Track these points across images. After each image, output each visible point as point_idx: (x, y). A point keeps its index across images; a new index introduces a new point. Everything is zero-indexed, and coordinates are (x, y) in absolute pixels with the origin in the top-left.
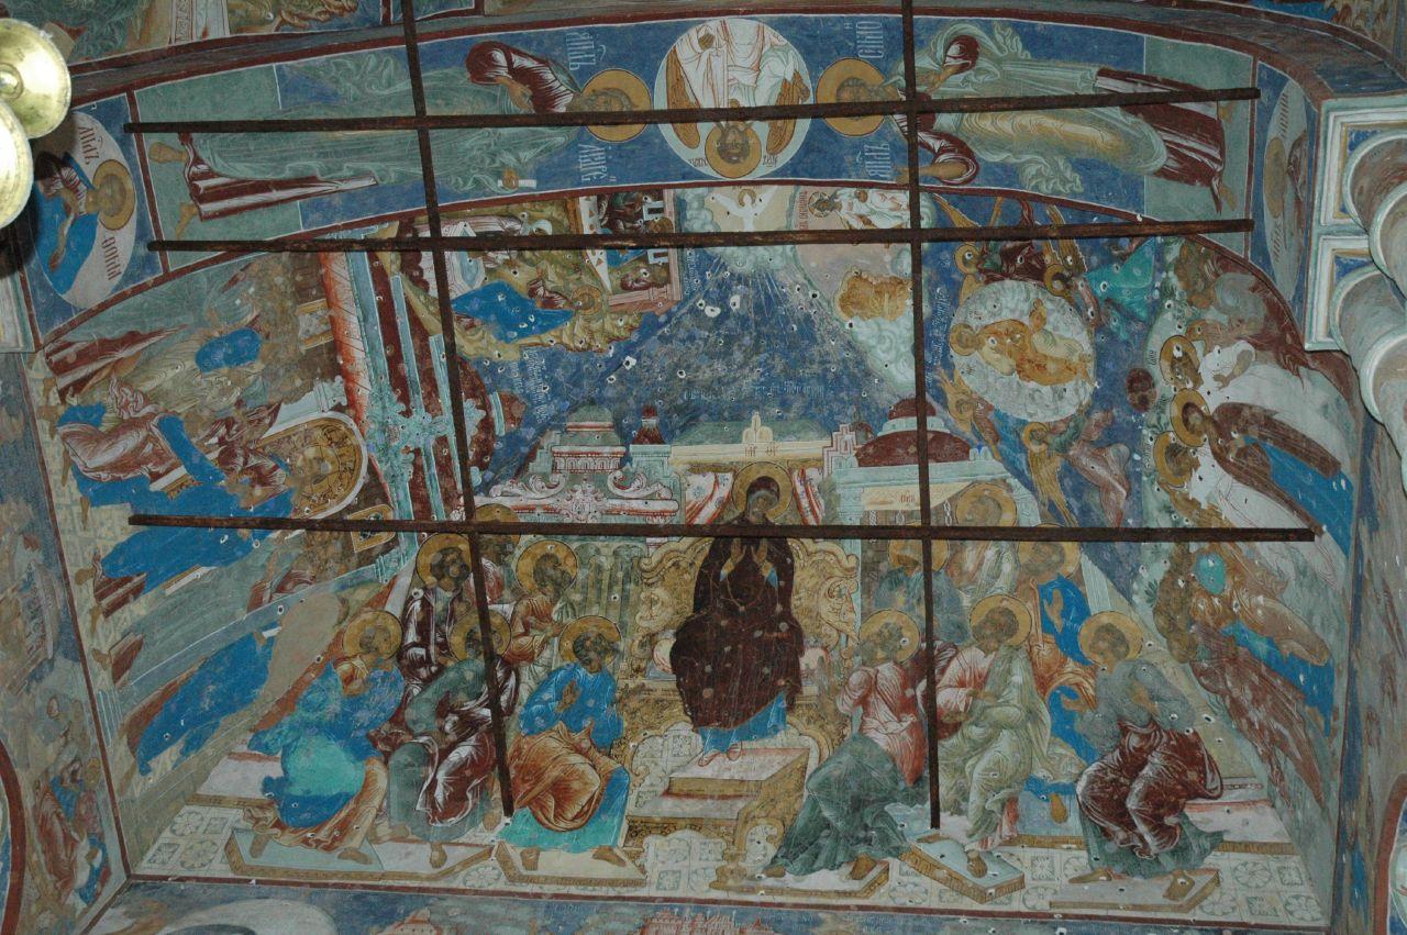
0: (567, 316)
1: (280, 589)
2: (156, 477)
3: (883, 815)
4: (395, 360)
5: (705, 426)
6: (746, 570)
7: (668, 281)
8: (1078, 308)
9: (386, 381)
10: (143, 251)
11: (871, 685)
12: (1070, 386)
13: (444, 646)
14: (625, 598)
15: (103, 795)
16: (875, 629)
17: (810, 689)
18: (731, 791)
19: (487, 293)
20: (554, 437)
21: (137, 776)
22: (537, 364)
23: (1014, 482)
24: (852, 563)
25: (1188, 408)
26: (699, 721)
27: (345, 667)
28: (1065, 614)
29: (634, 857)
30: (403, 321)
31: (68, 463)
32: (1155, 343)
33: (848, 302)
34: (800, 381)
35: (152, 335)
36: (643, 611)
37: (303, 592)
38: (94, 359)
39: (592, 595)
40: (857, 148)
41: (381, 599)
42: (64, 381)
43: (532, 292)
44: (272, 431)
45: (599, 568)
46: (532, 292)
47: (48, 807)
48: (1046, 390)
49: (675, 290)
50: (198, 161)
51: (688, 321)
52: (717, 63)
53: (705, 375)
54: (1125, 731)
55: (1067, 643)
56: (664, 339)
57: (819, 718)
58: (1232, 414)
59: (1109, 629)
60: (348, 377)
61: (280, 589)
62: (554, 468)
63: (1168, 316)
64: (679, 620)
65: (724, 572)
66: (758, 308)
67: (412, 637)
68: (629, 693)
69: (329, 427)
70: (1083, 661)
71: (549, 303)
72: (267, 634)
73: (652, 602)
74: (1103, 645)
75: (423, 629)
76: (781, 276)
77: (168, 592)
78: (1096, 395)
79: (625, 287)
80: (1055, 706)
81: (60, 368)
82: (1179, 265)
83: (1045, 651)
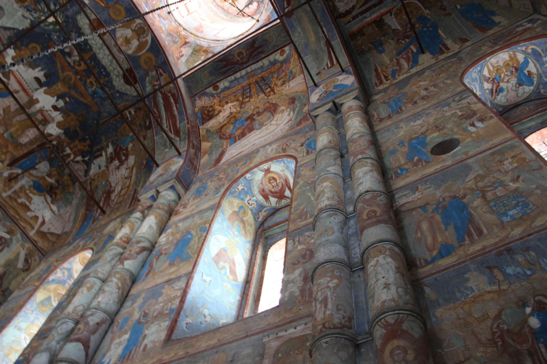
1: (445, 9)
2: (412, 52)
9: (381, 6)
15: (504, 31)
31: (406, 73)
35: (375, 65)
38: (380, 76)
42: (384, 81)
44: (400, 28)
47: (501, 43)
50: (324, 69)
60: (383, 15)
61: (445, 9)
69: (396, 15)
72: (459, 7)
77: (445, 37)
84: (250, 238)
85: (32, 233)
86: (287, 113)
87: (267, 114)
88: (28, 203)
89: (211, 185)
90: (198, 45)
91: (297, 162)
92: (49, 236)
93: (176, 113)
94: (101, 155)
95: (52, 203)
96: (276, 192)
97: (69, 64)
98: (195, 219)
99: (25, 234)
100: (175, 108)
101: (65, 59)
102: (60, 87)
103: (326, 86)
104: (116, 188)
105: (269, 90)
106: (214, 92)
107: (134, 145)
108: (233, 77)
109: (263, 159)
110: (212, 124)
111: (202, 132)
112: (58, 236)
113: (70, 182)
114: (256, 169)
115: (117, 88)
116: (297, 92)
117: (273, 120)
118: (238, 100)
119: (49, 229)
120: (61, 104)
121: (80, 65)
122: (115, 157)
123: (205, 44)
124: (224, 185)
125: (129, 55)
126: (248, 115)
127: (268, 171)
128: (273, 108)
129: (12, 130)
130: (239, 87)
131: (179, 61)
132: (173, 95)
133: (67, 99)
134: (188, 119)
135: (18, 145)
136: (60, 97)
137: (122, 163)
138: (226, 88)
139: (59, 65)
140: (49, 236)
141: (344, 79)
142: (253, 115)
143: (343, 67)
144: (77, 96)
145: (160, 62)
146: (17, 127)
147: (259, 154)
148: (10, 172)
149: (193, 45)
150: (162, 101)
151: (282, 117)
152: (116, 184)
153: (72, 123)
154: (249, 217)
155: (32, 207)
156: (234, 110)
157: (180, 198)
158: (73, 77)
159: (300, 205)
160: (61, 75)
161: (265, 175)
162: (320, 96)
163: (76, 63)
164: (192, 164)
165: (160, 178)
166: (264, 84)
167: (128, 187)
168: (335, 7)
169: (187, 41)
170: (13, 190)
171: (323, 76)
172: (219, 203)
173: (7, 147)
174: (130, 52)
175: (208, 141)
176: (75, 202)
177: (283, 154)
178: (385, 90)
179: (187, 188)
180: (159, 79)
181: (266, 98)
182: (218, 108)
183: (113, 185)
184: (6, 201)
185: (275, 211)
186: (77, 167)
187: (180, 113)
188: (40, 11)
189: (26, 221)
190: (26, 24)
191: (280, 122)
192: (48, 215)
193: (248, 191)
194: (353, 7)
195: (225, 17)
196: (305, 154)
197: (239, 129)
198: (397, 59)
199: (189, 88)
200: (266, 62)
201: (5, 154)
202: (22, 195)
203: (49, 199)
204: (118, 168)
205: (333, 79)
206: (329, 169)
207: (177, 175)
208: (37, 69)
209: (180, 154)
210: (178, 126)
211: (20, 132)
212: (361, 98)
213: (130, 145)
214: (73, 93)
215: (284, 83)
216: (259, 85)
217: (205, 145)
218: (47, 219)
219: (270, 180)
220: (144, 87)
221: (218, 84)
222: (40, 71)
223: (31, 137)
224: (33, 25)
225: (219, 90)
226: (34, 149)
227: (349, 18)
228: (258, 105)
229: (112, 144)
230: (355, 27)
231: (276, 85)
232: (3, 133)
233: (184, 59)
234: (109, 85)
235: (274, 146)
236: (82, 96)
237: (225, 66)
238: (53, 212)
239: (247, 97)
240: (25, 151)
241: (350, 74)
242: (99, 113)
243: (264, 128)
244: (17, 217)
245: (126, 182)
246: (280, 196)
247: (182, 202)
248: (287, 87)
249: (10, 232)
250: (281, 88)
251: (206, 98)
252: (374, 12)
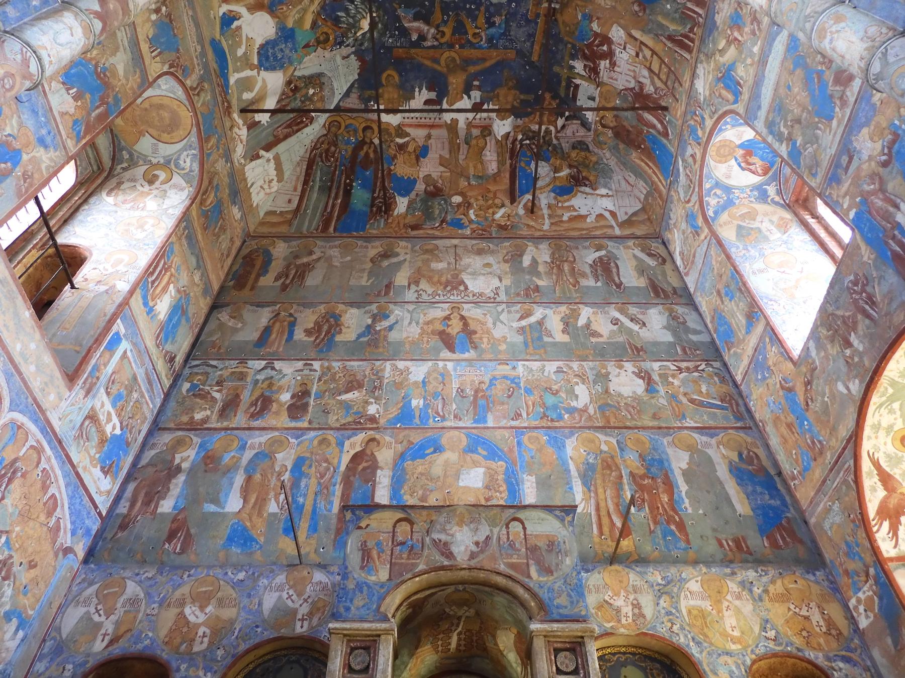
85: (617, 232)
88: (575, 214)
92: (634, 219)
94: (577, 87)
95: (595, 189)
97: (433, 47)
99: (611, 238)
102: (456, 81)
104: (641, 80)
107: (598, 18)
112: (643, 209)
113: (583, 153)
119: (626, 213)
120: (476, 95)
121: (443, 34)
122: (594, 63)
129: (472, 171)
133: (476, 83)
135: (495, 177)
136: (467, 90)
137: (610, 55)
139: (427, 63)
140: (634, 219)
144: (479, 68)
146: (471, 165)
148: (521, 206)
152: (634, 78)
153: (510, 99)
155: (583, 212)
158: (453, 54)
160: (441, 68)
163: (438, 36)
167: (654, 52)
170: (546, 216)
173: (489, 191)
176: (613, 162)
183: (632, 85)
184: (555, 231)
186: (569, 131)
188: (349, 30)
189: (596, 228)
190: (354, 62)
192: (608, 204)
201: (495, 197)
202: (559, 212)
203: (588, 190)
204: (613, 64)
208: (417, 93)
211: (479, 166)
214: (472, 69)
218: (611, 208)
222: (420, 92)
223: (495, 158)
224: (359, 55)
226: (511, 165)
229: (573, 60)
232: (469, 184)
236: (484, 60)
238: (607, 196)
240: (508, 176)
242: (520, 53)
244: (584, 232)
245: (644, 57)
249: (599, 248)
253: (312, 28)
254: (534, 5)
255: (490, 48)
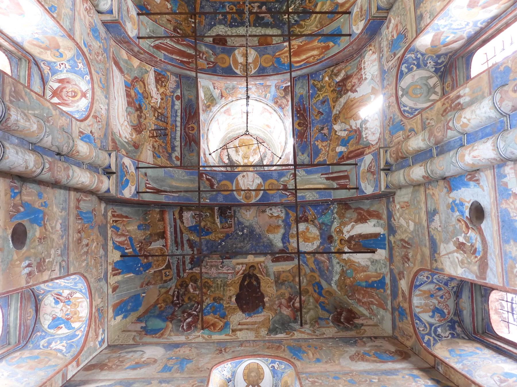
0: (211, 233)
1: (147, 284)
2: (127, 249)
3: (289, 325)
4: (176, 237)
5: (238, 257)
6: (250, 283)
7: (232, 227)
8: (316, 226)
9: (174, 242)
10: (135, 193)
11: (281, 304)
12: (315, 242)
13: (183, 300)
14: (224, 289)
15: (106, 320)
16: (279, 293)
17: (267, 305)
18: (255, 323)
19: (195, 226)
20: (207, 258)
21: (113, 319)
22: (204, 242)
23: (304, 265)
24: (272, 281)
25: (341, 240)
26: (244, 311)
27: (159, 305)
28: (318, 289)
29: (235, 335)
30: (178, 230)
31: (112, 237)
32: (333, 229)
33: (269, 231)
34: (259, 246)
36: (228, 292)
37: (151, 286)
39: (216, 289)
40: (272, 196)
41: (168, 291)
42: (114, 219)
43: (204, 227)
44: (150, 247)
45: (218, 284)
46: (204, 227)
47: (96, 314)
48: (310, 244)
49: (233, 229)
50: (147, 180)
51: (235, 236)
52: (245, 180)
53: (239, 246)
54: (336, 309)
55: (320, 294)
56: (231, 239)
57: (270, 309)
58: (351, 238)
59: (327, 291)
61: (147, 284)
62: (207, 265)
63: (335, 223)
64: (236, 293)
65: (245, 284)
66: (250, 232)
67: (175, 299)
68: (226, 307)
70: (324, 297)
71: (208, 230)
72: (143, 295)
73: (230, 290)
74: (327, 294)
75: (178, 297)
76: (255, 226)
78: (321, 243)
79: (223, 228)
80: (320, 305)
81: (113, 216)
82: (337, 213)
83: (316, 295)
84: (27, 46)
86: (128, 137)
87: (136, 122)
89: (96, 45)
90: (216, 104)
91: (77, 120)
93: (174, 57)
96: (61, 91)
97: (254, 3)
98: (69, 10)
100: (178, 58)
101: (259, 2)
103: (132, 175)
105: (155, 135)
106: (175, 95)
107: (168, 9)
108: (179, 114)
109: (96, 97)
110: (151, 78)
111: (148, 67)
114: (91, 86)
115: (218, 26)
116: (141, 153)
117: (129, 124)
118: (160, 108)
123: (215, 109)
124: (90, 53)
125: (235, 50)
126: (143, 108)
127: (84, 95)
128: (138, 129)
130: (169, 115)
131: (211, 83)
132: (188, 63)
134: (164, 62)
138: (173, 105)
141: (131, 190)
142: (141, 112)
143: (141, 194)
145: (218, 69)
147: (103, 97)
149: (217, 100)
150: (189, 52)
151: (127, 132)
154: (48, 56)
156: (153, 100)
157: (99, 12)
159: (29, 99)
161: (82, 92)
162: (126, 167)
163: (251, 8)
164: (124, 41)
165: (125, 8)
166: (161, 133)
168: (190, 210)
169: (223, 98)
171: (142, 176)
172: (73, 39)
174: (236, 52)
175: (139, 66)
177: (92, 114)
178: (105, 215)
179: (105, 23)
180: (206, 60)
181: (150, 129)
182: (162, 90)
185: (44, 82)
187: (172, 59)
191: (123, 128)
193: (73, 70)
194: (182, 222)
195: (229, 136)
196: (81, 130)
197: (136, 95)
198: (127, 235)
199: (188, 77)
200: (178, 143)
205: (135, 182)
206: (50, 137)
207: (120, 23)
209: (139, 38)
210: (163, 52)
212: (106, 195)
213: (169, 6)
215: (154, 147)
216: (162, 129)
217: (136, 63)
219: (75, 92)
220: (206, 45)
221: (180, 101)
225: (175, 99)
227: (177, 216)
228: (147, 120)
230: (168, 217)
231: (156, 141)
233: (211, 87)
234: (224, 22)
235: (104, 112)
237: (190, 114)
239: (158, 116)
241: (132, 196)
243: (126, 114)
246: (55, 93)
247: (93, 11)
248: (149, 148)
250: (151, 143)
251: (174, 86)
252: (171, 235)
253: (317, 4)
254: (202, 22)
255: (224, 2)
